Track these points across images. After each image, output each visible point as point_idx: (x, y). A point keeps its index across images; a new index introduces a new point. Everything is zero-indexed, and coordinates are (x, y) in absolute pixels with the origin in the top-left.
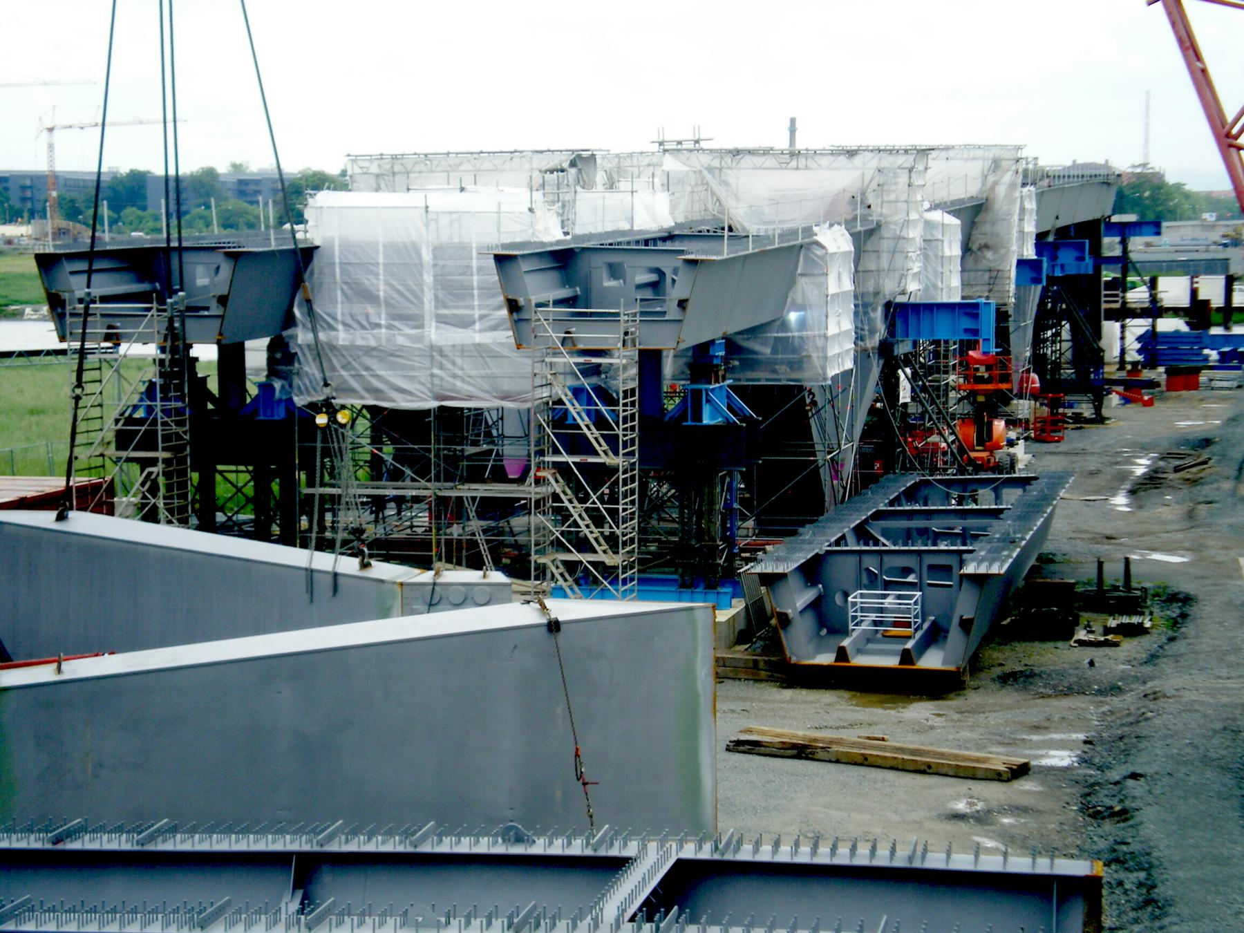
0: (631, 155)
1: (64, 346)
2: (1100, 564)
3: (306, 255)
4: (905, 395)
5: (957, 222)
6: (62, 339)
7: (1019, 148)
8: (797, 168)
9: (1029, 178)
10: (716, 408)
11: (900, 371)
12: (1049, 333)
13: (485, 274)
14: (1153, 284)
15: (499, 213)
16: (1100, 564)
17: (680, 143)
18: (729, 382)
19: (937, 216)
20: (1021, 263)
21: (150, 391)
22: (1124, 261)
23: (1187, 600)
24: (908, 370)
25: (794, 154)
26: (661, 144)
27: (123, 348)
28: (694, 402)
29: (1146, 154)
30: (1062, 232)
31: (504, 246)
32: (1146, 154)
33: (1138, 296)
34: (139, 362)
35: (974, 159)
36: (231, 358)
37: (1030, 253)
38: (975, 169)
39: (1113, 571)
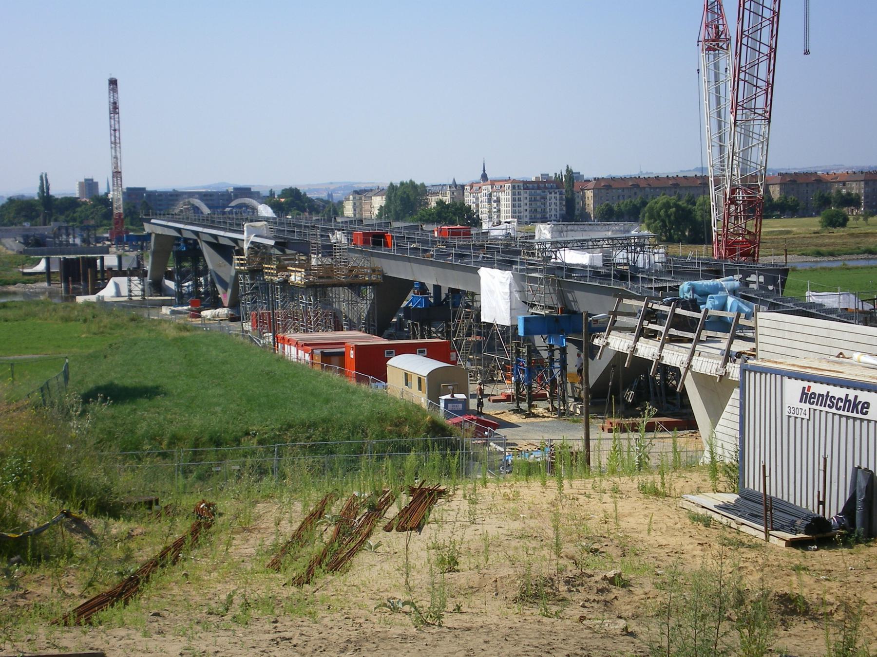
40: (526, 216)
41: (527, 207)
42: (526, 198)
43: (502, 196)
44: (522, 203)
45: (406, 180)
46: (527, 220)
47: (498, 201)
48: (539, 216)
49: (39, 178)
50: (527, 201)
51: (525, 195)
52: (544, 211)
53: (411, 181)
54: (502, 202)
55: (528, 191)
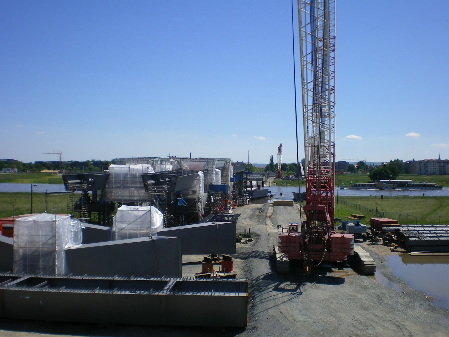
0: (164, 158)
1: (66, 191)
2: (245, 230)
3: (108, 175)
4: (212, 201)
5: (220, 171)
6: (66, 190)
7: (230, 159)
8: (194, 161)
9: (233, 164)
10: (180, 203)
11: (212, 196)
12: (235, 190)
13: (140, 180)
14: (251, 182)
15: (142, 168)
16: (245, 230)
17: (173, 156)
18: (183, 198)
19: (217, 170)
20: (231, 178)
21: (80, 200)
22: (247, 178)
23: (259, 235)
24: (213, 196)
25: (191, 159)
26: (169, 156)
27: (76, 192)
28: (176, 201)
29: (249, 161)
30: (237, 173)
31: (143, 174)
32: (249, 161)
33: (249, 184)
34: (78, 195)
35: (223, 161)
36: (95, 194)
37: (232, 177)
38: (223, 162)
39: (247, 231)
40: (438, 173)
41: (438, 169)
42: (438, 166)
43: (429, 166)
44: (436, 168)
45: (396, 159)
46: (438, 174)
47: (427, 167)
48: (443, 173)
49: (270, 157)
50: (438, 167)
51: (437, 165)
52: (445, 171)
53: (398, 159)
54: (429, 168)
55: (439, 164)
